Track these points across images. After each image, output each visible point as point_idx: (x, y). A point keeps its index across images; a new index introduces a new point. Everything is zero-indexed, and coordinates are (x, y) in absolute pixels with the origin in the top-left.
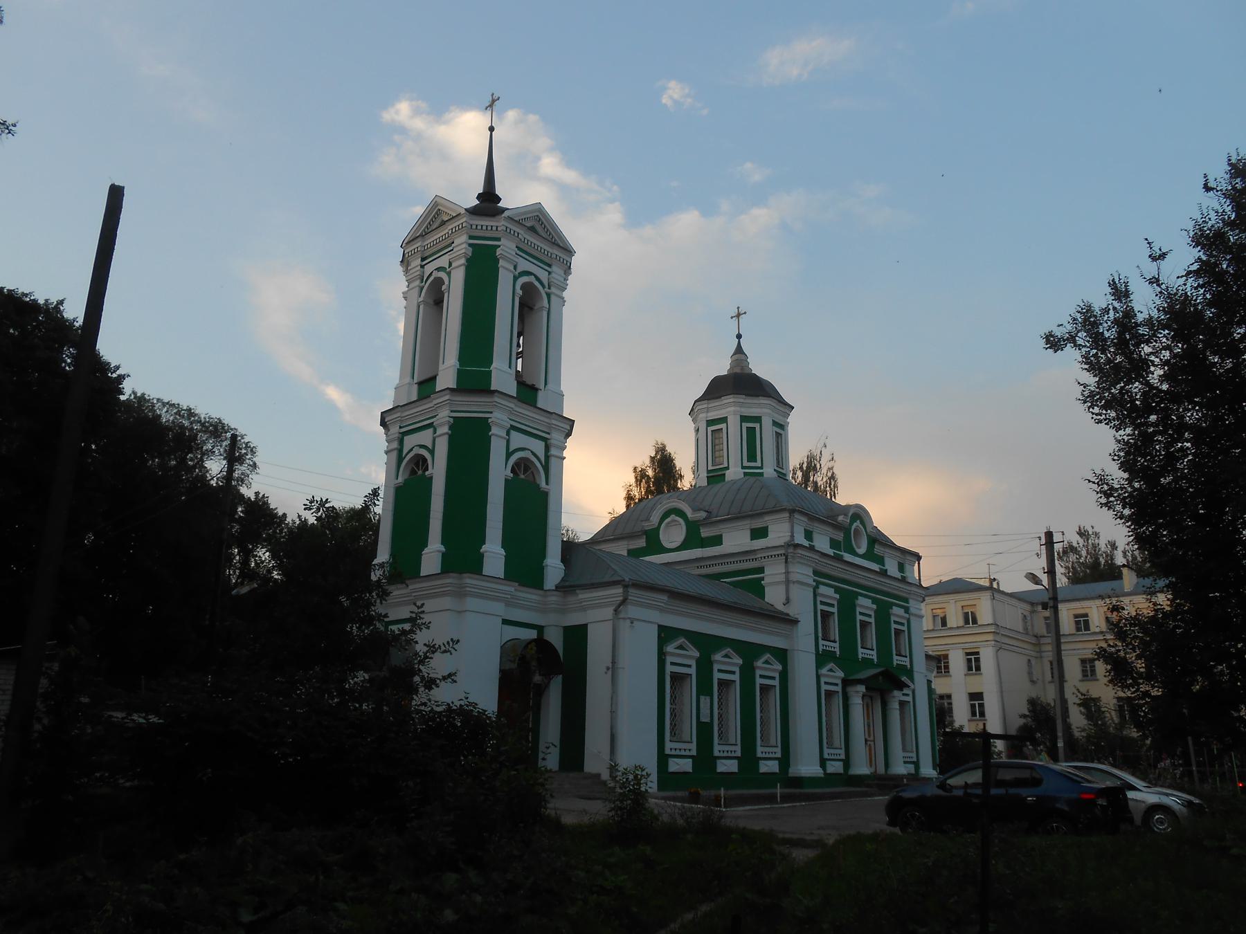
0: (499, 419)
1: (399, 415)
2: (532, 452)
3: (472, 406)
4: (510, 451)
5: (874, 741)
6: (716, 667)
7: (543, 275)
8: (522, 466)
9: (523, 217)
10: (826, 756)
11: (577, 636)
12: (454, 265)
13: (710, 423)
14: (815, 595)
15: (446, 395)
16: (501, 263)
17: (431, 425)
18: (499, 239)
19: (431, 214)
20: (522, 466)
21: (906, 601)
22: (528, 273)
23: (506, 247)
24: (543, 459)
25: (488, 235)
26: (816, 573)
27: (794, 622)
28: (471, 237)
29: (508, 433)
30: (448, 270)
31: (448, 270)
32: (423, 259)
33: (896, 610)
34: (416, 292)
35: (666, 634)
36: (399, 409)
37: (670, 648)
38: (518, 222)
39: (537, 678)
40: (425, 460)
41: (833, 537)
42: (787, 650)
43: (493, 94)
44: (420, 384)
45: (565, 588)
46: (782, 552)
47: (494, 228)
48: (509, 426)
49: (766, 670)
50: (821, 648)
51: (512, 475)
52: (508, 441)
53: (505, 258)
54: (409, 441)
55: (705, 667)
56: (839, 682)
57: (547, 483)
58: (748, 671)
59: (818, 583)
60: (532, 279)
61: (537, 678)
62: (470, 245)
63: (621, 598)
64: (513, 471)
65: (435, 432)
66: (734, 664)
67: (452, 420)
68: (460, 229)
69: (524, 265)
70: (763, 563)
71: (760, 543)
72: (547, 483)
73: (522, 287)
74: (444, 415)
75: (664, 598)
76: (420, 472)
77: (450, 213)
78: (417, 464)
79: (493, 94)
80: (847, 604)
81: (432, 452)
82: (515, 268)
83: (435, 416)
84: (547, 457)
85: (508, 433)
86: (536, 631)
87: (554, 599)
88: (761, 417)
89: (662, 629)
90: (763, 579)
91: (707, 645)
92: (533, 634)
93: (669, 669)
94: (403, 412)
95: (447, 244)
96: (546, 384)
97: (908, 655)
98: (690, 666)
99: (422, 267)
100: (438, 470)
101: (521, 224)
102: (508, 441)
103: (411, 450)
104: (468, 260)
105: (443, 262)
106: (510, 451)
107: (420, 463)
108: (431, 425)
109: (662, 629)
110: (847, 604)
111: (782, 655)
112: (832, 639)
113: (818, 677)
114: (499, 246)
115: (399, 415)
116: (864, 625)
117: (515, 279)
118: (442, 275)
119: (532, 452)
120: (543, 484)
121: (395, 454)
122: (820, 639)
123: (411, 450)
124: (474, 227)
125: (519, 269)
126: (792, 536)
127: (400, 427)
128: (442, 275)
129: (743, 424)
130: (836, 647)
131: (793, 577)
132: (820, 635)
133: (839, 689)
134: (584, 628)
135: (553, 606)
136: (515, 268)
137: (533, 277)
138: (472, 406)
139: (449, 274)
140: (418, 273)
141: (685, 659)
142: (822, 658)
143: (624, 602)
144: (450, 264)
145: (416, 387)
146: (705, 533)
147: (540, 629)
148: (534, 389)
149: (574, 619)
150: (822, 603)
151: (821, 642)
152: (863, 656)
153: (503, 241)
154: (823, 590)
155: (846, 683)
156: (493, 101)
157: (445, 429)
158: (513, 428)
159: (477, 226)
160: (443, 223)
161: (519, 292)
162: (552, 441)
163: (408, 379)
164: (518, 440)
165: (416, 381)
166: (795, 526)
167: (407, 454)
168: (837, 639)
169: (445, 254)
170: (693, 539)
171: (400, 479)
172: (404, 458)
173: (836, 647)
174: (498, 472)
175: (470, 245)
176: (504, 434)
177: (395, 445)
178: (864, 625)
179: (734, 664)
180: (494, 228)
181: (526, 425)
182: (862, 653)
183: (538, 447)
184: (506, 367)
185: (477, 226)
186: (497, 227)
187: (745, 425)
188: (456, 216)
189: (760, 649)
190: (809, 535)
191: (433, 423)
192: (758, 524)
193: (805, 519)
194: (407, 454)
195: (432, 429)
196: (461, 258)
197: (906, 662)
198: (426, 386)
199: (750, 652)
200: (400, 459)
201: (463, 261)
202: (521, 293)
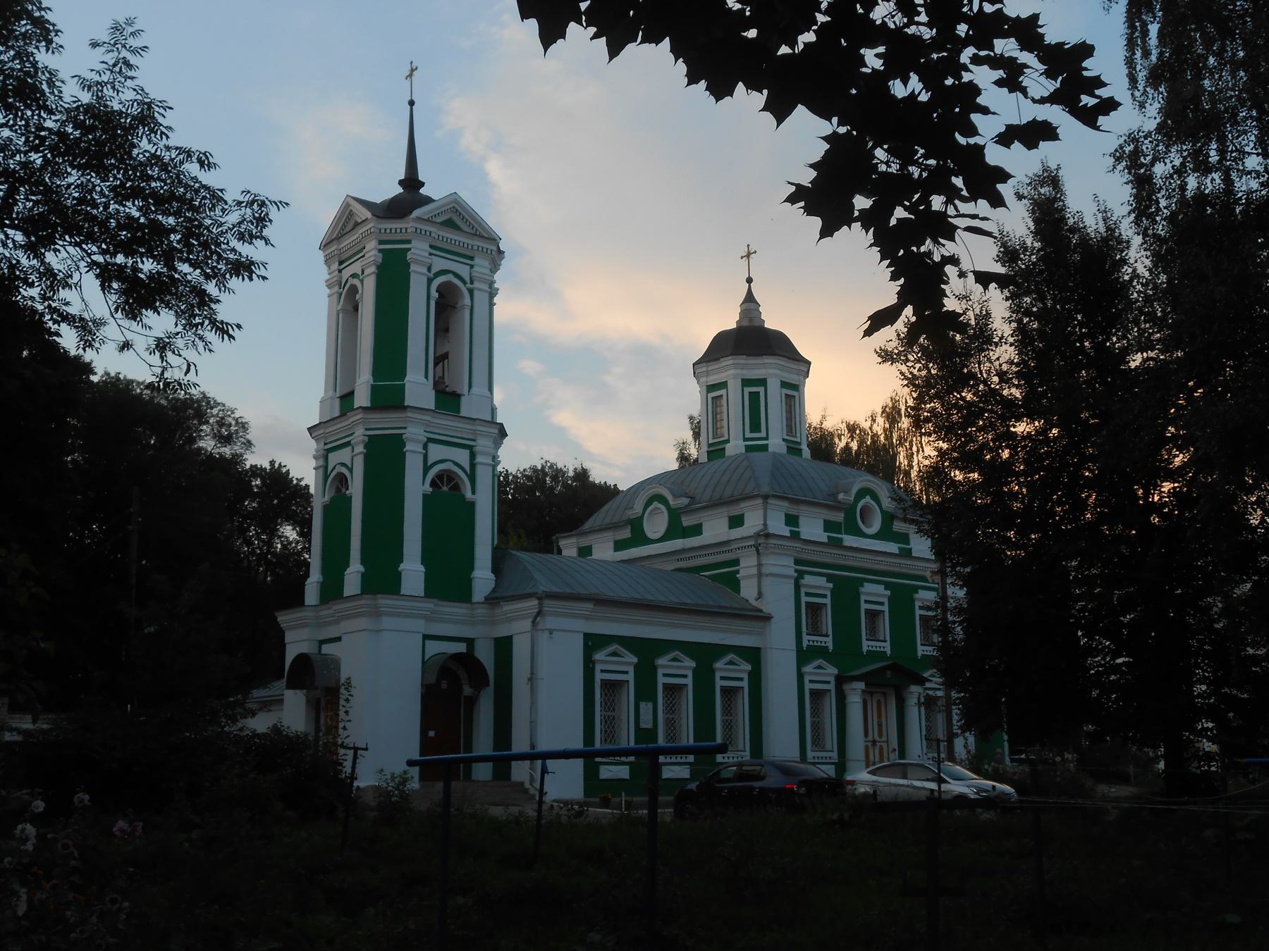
0: (414, 434)
1: (321, 431)
2: (451, 461)
3: (386, 423)
4: (429, 464)
5: (887, 742)
7: (464, 271)
9: (433, 214)
11: (504, 646)
12: (366, 272)
14: (797, 587)
15: (358, 414)
16: (413, 267)
17: (348, 444)
18: (409, 242)
19: (344, 215)
23: (418, 250)
24: (468, 468)
25: (398, 237)
26: (797, 562)
27: (768, 618)
28: (381, 242)
29: (425, 447)
30: (361, 278)
31: (361, 278)
32: (341, 263)
34: (335, 297)
35: (593, 643)
36: (322, 425)
37: (599, 656)
38: (428, 220)
39: (467, 690)
40: (346, 479)
42: (759, 649)
43: (412, 63)
44: (342, 398)
45: (493, 600)
46: (752, 543)
47: (404, 231)
48: (425, 439)
49: (729, 672)
50: (805, 645)
51: (431, 489)
53: (418, 262)
54: (335, 458)
55: (646, 674)
56: (832, 679)
57: (473, 493)
58: (704, 677)
59: (801, 574)
60: (450, 277)
61: (467, 690)
62: (380, 251)
63: (537, 610)
64: (433, 484)
65: (353, 452)
66: (685, 668)
68: (369, 234)
69: (439, 264)
70: (739, 554)
71: (737, 533)
72: (473, 493)
74: (359, 434)
75: (590, 606)
77: (361, 216)
78: (341, 482)
79: (412, 63)
80: (846, 592)
81: (351, 470)
82: (429, 269)
83: (352, 434)
84: (473, 465)
86: (465, 644)
87: (481, 611)
89: (587, 636)
90: (738, 572)
91: (647, 651)
92: (461, 648)
93: (599, 676)
94: (326, 428)
95: (359, 248)
96: (470, 387)
98: (627, 673)
99: (340, 271)
100: (356, 489)
101: (430, 221)
103: (334, 468)
104: (378, 268)
105: (356, 268)
106: (429, 464)
107: (342, 481)
108: (348, 444)
109: (587, 636)
110: (846, 592)
111: (753, 655)
112: (824, 633)
114: (410, 249)
115: (321, 431)
116: (873, 616)
117: (430, 281)
118: (356, 282)
120: (469, 495)
121: (321, 471)
122: (804, 634)
123: (334, 468)
124: (383, 231)
125: (434, 270)
126: (765, 525)
127: (325, 444)
128: (356, 282)
129: (745, 388)
130: (829, 642)
131: (765, 570)
133: (832, 687)
134: (509, 639)
135: (480, 618)
136: (429, 269)
137: (451, 275)
138: (386, 423)
139: (362, 281)
140: (335, 279)
141: (624, 666)
142: (805, 656)
143: (539, 613)
144: (363, 273)
145: (337, 402)
146: (687, 521)
147: (470, 642)
148: (457, 396)
149: (502, 632)
150: (807, 594)
152: (870, 648)
153: (414, 244)
154: (808, 580)
155: (841, 680)
156: (412, 70)
157: (360, 449)
158: (430, 440)
159: (385, 230)
160: (357, 224)
161: (435, 295)
162: (477, 449)
163: (331, 393)
164: (436, 452)
165: (338, 396)
166: (769, 511)
167: (332, 472)
168: (830, 632)
169: (358, 260)
170: (675, 530)
171: (327, 498)
172: (330, 474)
173: (829, 642)
174: (415, 487)
175: (380, 251)
176: (420, 449)
177: (321, 462)
178: (873, 616)
179: (685, 668)
180: (404, 231)
181: (447, 436)
182: (866, 645)
183: (462, 457)
184: (422, 379)
185: (385, 230)
186: (406, 229)
187: (747, 390)
188: (362, 222)
189: (719, 650)
190: (792, 520)
191: (350, 441)
192: (735, 511)
194: (332, 472)
195: (350, 448)
196: (371, 266)
198: (347, 398)
199: (705, 655)
200: (326, 477)
201: (372, 269)
202: (437, 295)
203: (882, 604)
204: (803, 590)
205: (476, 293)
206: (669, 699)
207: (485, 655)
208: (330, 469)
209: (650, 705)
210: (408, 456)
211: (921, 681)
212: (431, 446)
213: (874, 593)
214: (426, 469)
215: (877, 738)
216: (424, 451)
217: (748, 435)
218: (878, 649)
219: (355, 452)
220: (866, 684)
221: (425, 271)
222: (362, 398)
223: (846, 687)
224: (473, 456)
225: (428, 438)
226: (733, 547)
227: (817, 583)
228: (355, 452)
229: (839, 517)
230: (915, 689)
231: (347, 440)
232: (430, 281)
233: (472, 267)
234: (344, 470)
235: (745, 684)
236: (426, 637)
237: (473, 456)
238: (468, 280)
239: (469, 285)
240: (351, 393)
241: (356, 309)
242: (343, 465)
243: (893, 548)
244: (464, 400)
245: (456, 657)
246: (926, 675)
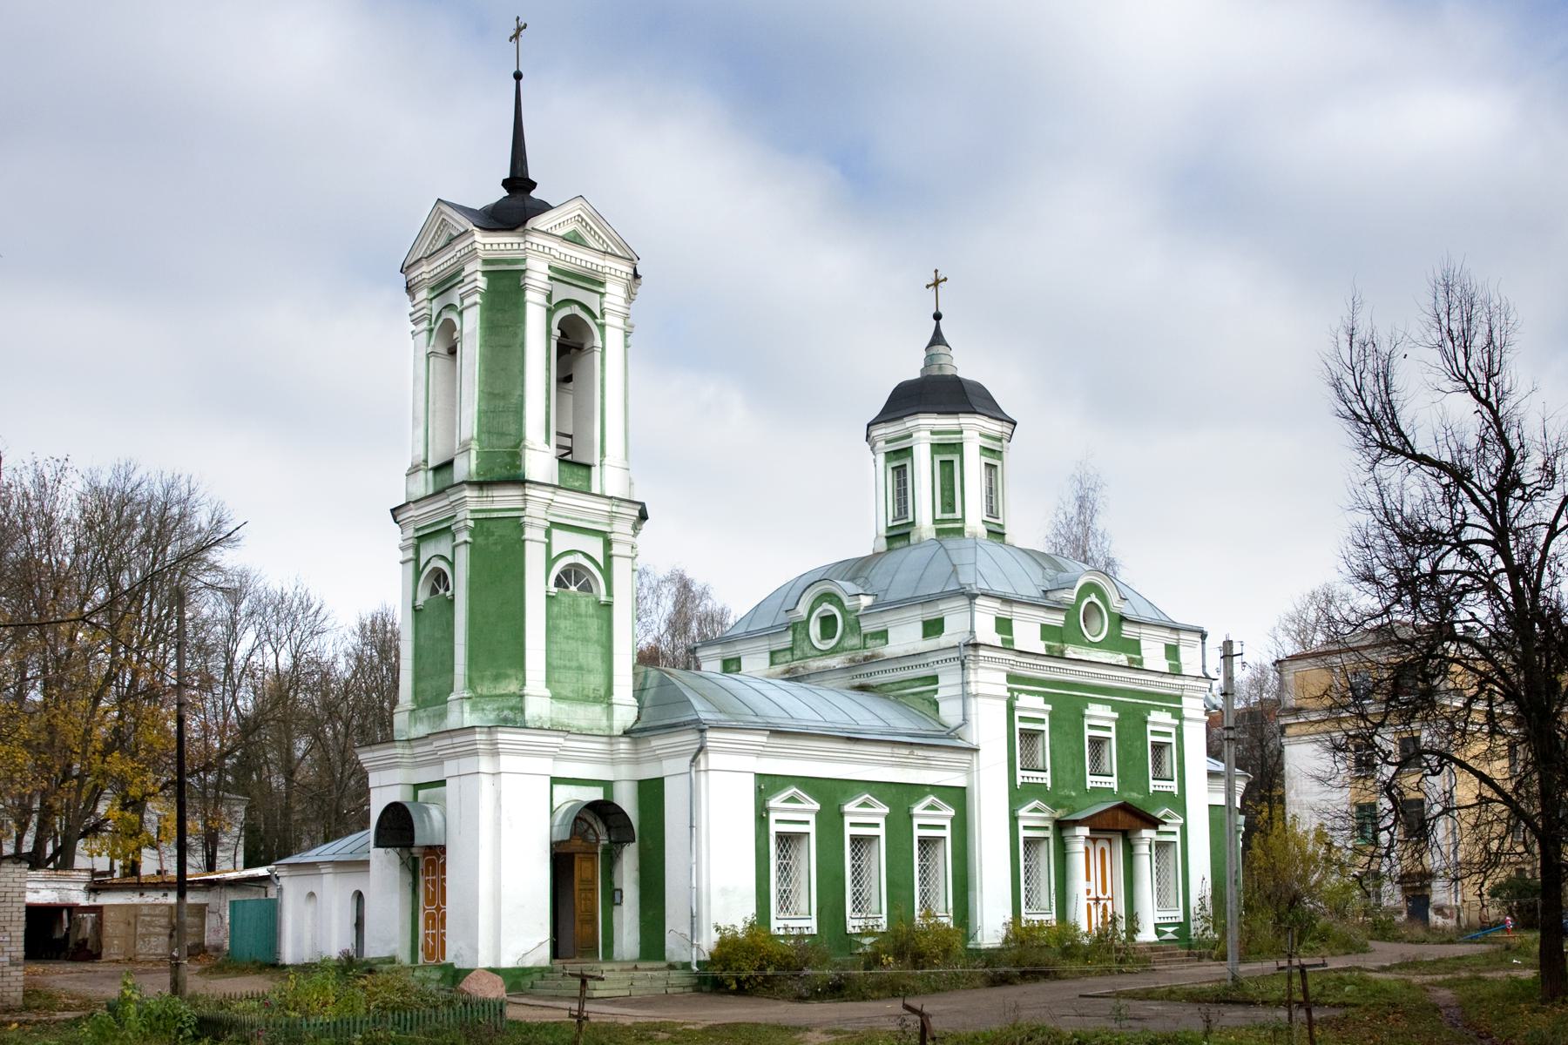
4: (554, 554)
6: (848, 820)
8: (571, 576)
11: (651, 792)
14: (1011, 709)
21: (1178, 699)
22: (567, 302)
26: (1012, 678)
27: (974, 750)
29: (548, 534)
33: (1154, 716)
35: (767, 785)
41: (1046, 622)
42: (964, 788)
46: (956, 655)
49: (930, 818)
50: (1019, 783)
52: (549, 546)
56: (1049, 824)
63: (698, 746)
64: (559, 582)
65: (454, 540)
71: (932, 643)
76: (442, 591)
78: (437, 580)
81: (452, 564)
84: (609, 558)
87: (624, 745)
89: (760, 777)
90: (936, 691)
91: (831, 794)
92: (596, 794)
93: (774, 828)
98: (807, 822)
102: (549, 546)
103: (428, 562)
106: (554, 554)
107: (439, 578)
111: (958, 797)
113: (1014, 819)
116: (1097, 743)
121: (411, 565)
123: (428, 562)
130: (1046, 778)
131: (972, 689)
134: (658, 783)
135: (622, 756)
142: (1018, 795)
143: (701, 749)
147: (607, 785)
149: (649, 772)
150: (1022, 719)
151: (1019, 773)
154: (1024, 701)
155: (1061, 826)
164: (562, 541)
166: (976, 614)
173: (1046, 778)
176: (541, 535)
177: (410, 554)
178: (1097, 743)
181: (572, 519)
182: (1091, 781)
191: (450, 527)
193: (996, 604)
197: (1173, 787)
199: (901, 796)
200: (418, 573)
203: (1108, 729)
204: (1017, 714)
206: (857, 854)
207: (626, 800)
208: (422, 563)
211: (1154, 823)
212: (556, 533)
213: (1100, 715)
214: (550, 562)
216: (547, 540)
219: (457, 542)
220: (1091, 830)
224: (608, 544)
225: (551, 522)
226: (930, 660)
227: (1033, 705)
228: (457, 542)
229: (1058, 619)
230: (1148, 834)
231: (445, 525)
234: (443, 565)
235: (947, 833)
236: (555, 781)
237: (608, 544)
238: (598, 314)
239: (599, 321)
241: (452, 352)
242: (443, 558)
243: (1122, 659)
244: (595, 471)
245: (593, 806)
246: (1159, 815)
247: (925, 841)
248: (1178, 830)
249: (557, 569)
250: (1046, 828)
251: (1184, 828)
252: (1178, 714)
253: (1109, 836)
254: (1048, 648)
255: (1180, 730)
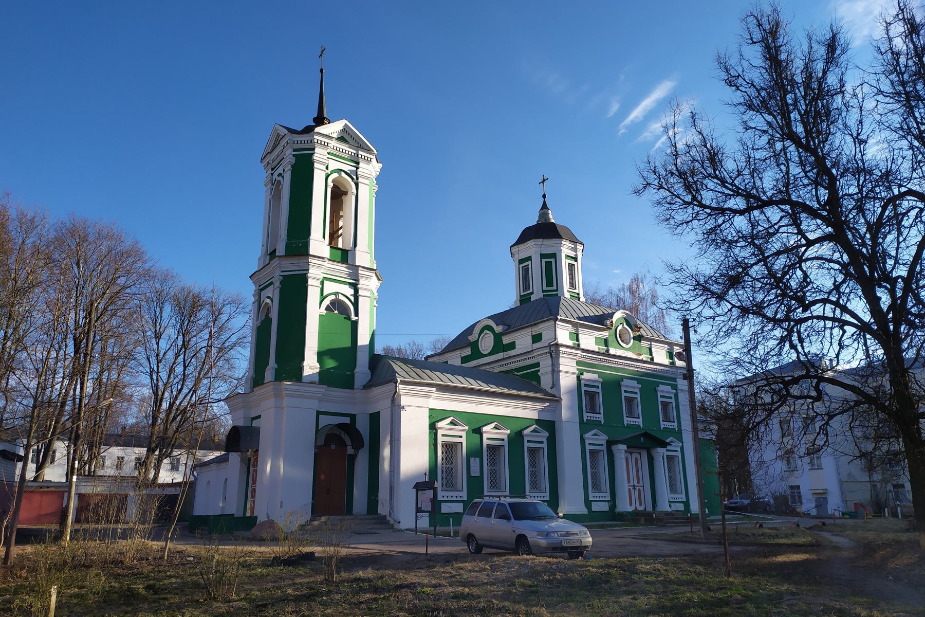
4: (325, 294)
10: (591, 498)
13: (521, 261)
15: (276, 262)
16: (316, 165)
20: (337, 305)
23: (320, 154)
26: (578, 363)
29: (322, 283)
39: (350, 451)
42: (554, 422)
44: (270, 254)
45: (367, 386)
47: (309, 142)
50: (585, 420)
51: (325, 312)
61: (350, 451)
62: (294, 155)
67: (281, 278)
73: (333, 181)
84: (356, 295)
85: (322, 283)
88: (556, 253)
90: (539, 371)
92: (347, 420)
97: (676, 421)
99: (272, 174)
104: (292, 166)
108: (272, 283)
112: (598, 411)
113: (582, 440)
116: (630, 401)
117: (327, 176)
119: (342, 294)
122: (584, 412)
124: (296, 142)
125: (330, 169)
127: (260, 286)
128: (280, 178)
130: (601, 417)
132: (584, 409)
133: (604, 448)
136: (327, 168)
139: (283, 177)
142: (585, 426)
144: (284, 170)
145: (268, 256)
146: (506, 340)
147: (353, 417)
151: (585, 414)
152: (629, 423)
153: (317, 150)
155: (610, 444)
161: (330, 184)
164: (330, 287)
170: (499, 347)
173: (601, 417)
175: (294, 155)
176: (318, 283)
178: (630, 401)
180: (309, 142)
182: (627, 420)
196: (288, 165)
197: (675, 425)
198: (272, 254)
201: (290, 167)
203: (636, 393)
205: (360, 184)
207: (363, 426)
209: (478, 460)
210: (310, 288)
211: (664, 444)
214: (323, 298)
215: (636, 484)
217: (545, 288)
218: (634, 423)
221: (324, 168)
222: (281, 250)
223: (614, 448)
231: (270, 281)
232: (327, 176)
233: (357, 168)
235: (545, 446)
236: (319, 413)
240: (275, 251)
242: (269, 297)
245: (341, 426)
246: (668, 441)
247: (532, 450)
248: (679, 449)
249: (327, 302)
250: (602, 445)
251: (682, 448)
252: (675, 387)
253: (639, 451)
254: (599, 348)
255: (676, 395)
